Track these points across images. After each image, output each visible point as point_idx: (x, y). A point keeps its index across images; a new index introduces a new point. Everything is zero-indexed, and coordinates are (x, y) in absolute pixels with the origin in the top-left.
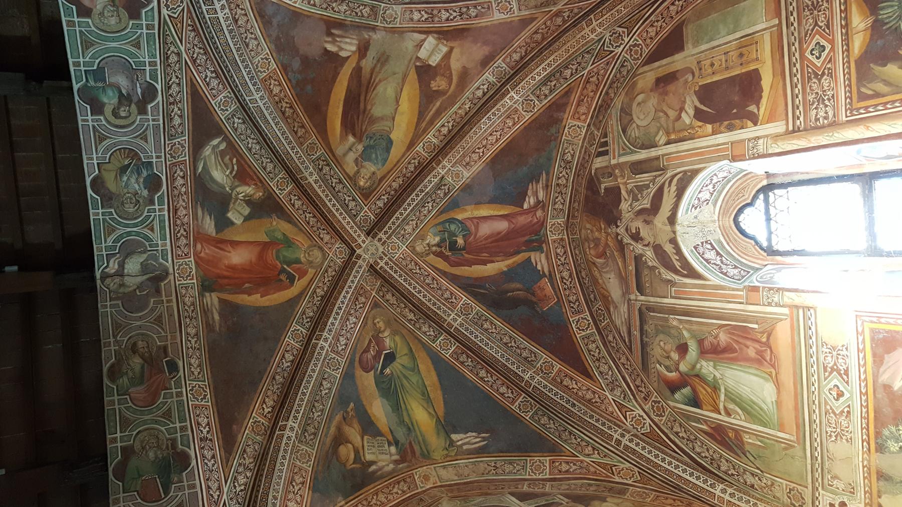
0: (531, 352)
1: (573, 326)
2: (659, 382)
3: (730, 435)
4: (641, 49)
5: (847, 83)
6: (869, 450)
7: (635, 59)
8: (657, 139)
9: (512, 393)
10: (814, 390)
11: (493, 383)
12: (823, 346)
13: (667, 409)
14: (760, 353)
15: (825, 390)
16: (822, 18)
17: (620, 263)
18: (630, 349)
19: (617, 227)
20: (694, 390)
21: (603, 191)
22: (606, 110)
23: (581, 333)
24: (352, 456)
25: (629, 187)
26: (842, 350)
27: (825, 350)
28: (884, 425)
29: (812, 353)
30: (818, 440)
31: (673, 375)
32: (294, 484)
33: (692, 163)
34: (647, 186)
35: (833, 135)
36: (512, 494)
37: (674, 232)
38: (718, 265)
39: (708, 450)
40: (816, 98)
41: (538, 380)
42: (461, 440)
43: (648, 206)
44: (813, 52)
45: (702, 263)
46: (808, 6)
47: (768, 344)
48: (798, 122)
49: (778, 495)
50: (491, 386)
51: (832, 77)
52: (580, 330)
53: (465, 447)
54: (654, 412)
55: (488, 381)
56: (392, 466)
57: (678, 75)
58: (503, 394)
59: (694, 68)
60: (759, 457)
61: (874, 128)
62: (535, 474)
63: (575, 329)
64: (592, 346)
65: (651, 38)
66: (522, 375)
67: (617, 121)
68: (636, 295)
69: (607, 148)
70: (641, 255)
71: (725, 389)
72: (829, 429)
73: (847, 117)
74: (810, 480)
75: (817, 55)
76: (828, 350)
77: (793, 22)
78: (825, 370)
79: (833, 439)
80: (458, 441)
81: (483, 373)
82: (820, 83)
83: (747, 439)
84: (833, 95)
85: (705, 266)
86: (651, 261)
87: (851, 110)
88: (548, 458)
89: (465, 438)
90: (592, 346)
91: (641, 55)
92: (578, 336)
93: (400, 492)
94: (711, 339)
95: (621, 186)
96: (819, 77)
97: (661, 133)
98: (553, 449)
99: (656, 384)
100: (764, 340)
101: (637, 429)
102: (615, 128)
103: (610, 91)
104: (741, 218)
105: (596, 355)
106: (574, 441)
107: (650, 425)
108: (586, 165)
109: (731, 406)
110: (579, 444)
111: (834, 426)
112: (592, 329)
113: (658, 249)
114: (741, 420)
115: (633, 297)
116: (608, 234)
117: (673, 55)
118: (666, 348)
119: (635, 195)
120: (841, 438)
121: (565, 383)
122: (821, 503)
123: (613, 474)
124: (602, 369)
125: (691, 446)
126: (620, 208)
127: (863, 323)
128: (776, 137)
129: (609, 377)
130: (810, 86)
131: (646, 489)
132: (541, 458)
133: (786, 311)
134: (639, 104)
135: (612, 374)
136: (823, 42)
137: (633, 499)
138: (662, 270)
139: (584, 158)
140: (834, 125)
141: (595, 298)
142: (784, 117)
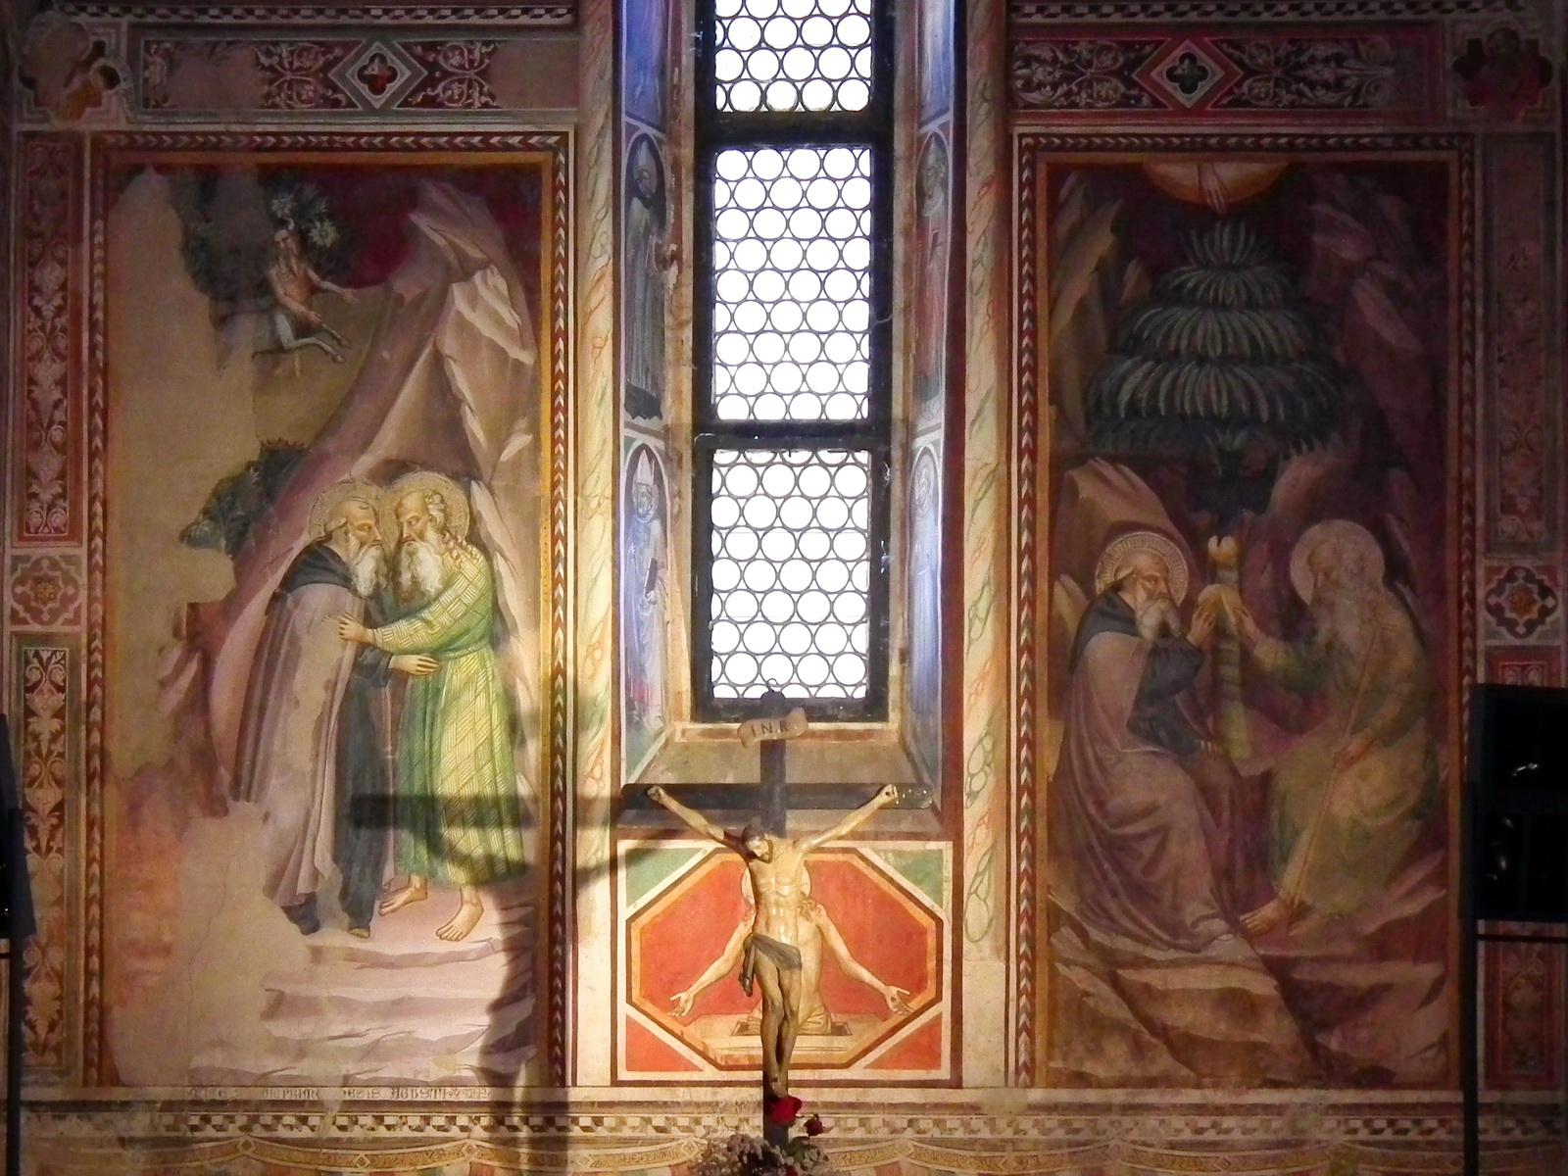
5: (1098, 141)
6: (259, 149)
10: (374, 12)
12: (486, 44)
15: (377, 43)
16: (1260, 88)
26: (481, 93)
29: (467, 12)
30: (250, 20)
35: (986, 100)
40: (1079, 61)
44: (1187, 62)
46: (1300, 52)
51: (1117, 105)
61: (985, 200)
72: (284, 50)
73: (1021, 136)
75: (1179, 72)
76: (477, 55)
77: (1275, 10)
78: (430, 47)
79: (263, 59)
82: (1111, 73)
84: (1075, 105)
87: (1034, 149)
96: (1123, 74)
111: (296, 64)
120: (271, 82)
122: (94, 19)
127: (548, 148)
130: (1108, 48)
136: (1203, 88)
140: (1008, 105)
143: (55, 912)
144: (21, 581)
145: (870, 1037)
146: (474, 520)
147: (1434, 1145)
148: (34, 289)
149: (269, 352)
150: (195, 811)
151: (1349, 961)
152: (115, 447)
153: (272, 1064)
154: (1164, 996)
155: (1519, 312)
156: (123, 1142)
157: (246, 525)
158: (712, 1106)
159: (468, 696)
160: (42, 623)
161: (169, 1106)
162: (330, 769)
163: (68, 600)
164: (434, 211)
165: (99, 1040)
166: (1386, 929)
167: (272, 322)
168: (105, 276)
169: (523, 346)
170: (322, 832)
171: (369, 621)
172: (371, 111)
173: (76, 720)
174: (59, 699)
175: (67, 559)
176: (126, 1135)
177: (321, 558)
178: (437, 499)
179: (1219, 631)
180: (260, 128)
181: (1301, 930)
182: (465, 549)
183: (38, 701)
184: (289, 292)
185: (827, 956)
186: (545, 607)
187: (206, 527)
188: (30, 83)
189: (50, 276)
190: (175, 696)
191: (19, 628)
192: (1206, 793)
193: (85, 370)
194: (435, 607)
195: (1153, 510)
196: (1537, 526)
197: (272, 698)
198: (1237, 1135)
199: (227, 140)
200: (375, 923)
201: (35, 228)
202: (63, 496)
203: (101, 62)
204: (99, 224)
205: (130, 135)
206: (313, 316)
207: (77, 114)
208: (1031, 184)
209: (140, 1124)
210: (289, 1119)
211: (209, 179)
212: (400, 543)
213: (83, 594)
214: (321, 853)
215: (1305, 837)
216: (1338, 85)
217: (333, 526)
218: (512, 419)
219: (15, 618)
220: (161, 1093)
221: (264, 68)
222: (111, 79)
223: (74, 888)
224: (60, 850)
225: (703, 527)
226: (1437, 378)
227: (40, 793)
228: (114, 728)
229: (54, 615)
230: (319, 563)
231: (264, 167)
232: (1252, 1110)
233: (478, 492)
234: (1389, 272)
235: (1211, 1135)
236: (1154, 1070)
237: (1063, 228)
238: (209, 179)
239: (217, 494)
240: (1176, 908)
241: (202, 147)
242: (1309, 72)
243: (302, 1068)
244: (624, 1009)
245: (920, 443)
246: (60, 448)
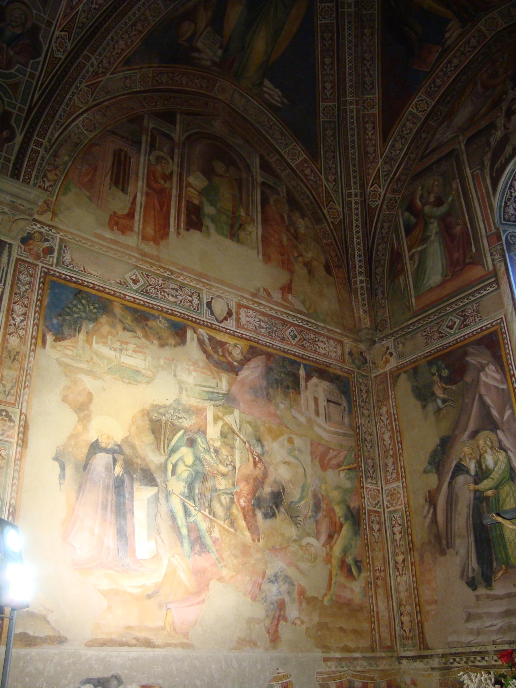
0: (372, 83)
1: (416, 100)
3: (399, 266)
9: (331, 94)
11: (327, 74)
12: (476, 304)
13: (395, 211)
17: (483, 110)
18: (423, 158)
23: (414, 109)
24: (188, 35)
26: (478, 317)
31: (419, 203)
32: (134, 28)
36: (262, 157)
38: (511, 195)
39: (383, 255)
41: (353, 108)
42: (269, 88)
45: (507, 183)
50: (324, 75)
52: (416, 107)
53: (266, 96)
54: (388, 202)
55: (325, 69)
56: (209, 63)
58: (324, 88)
62: (288, 156)
63: (414, 102)
64: (409, 125)
66: (348, 94)
72: (428, 329)
74: (395, 330)
76: (475, 307)
79: (424, 334)
80: (266, 87)
81: (328, 60)
83: (401, 278)
85: (505, 188)
86: (494, 139)
88: (305, 156)
89: (272, 90)
90: (409, 125)
92: (410, 109)
93: (199, 85)
98: (314, 155)
100: (467, 261)
101: (369, 198)
105: (405, 132)
106: (330, 163)
107: (378, 205)
109: (416, 258)
110: (330, 168)
112: (423, 115)
114: (411, 269)
115: (461, 138)
120: (426, 339)
121: (367, 126)
123: (327, 205)
124: (396, 144)
125: (380, 242)
129: (394, 154)
131: (332, 233)
132: (301, 151)
133: (491, 268)
135: (397, 155)
137: (318, 231)
138: (489, 154)
143: (406, 594)
144: (387, 496)
146: (500, 441)
148: (381, 415)
149: (436, 412)
150: (438, 555)
152: (405, 451)
153: (470, 638)
157: (439, 463)
159: (508, 499)
160: (394, 507)
162: (472, 533)
163: (399, 498)
167: (436, 402)
168: (396, 406)
169: (503, 383)
170: (473, 555)
171: (476, 483)
172: (451, 335)
173: (405, 532)
174: (400, 528)
175: (397, 487)
176: (433, 667)
177: (460, 467)
178: (488, 439)
180: (426, 352)
182: (499, 452)
184: (439, 393)
188: (374, 363)
189: (384, 410)
190: (428, 520)
191: (389, 510)
193: (395, 432)
194: (494, 473)
197: (453, 514)
199: (419, 358)
200: (493, 584)
201: (379, 399)
202: (394, 469)
203: (389, 351)
204: (393, 392)
205: (397, 367)
206: (446, 397)
207: (385, 367)
209: (435, 663)
212: (481, 455)
213: (402, 495)
214: (474, 563)
217: (461, 456)
218: (505, 406)
221: (424, 336)
222: (391, 354)
223: (410, 585)
224: (405, 574)
227: (398, 557)
229: (396, 503)
231: (428, 361)
233: (499, 432)
239: (431, 457)
241: (414, 362)
243: (481, 639)
246: (392, 456)
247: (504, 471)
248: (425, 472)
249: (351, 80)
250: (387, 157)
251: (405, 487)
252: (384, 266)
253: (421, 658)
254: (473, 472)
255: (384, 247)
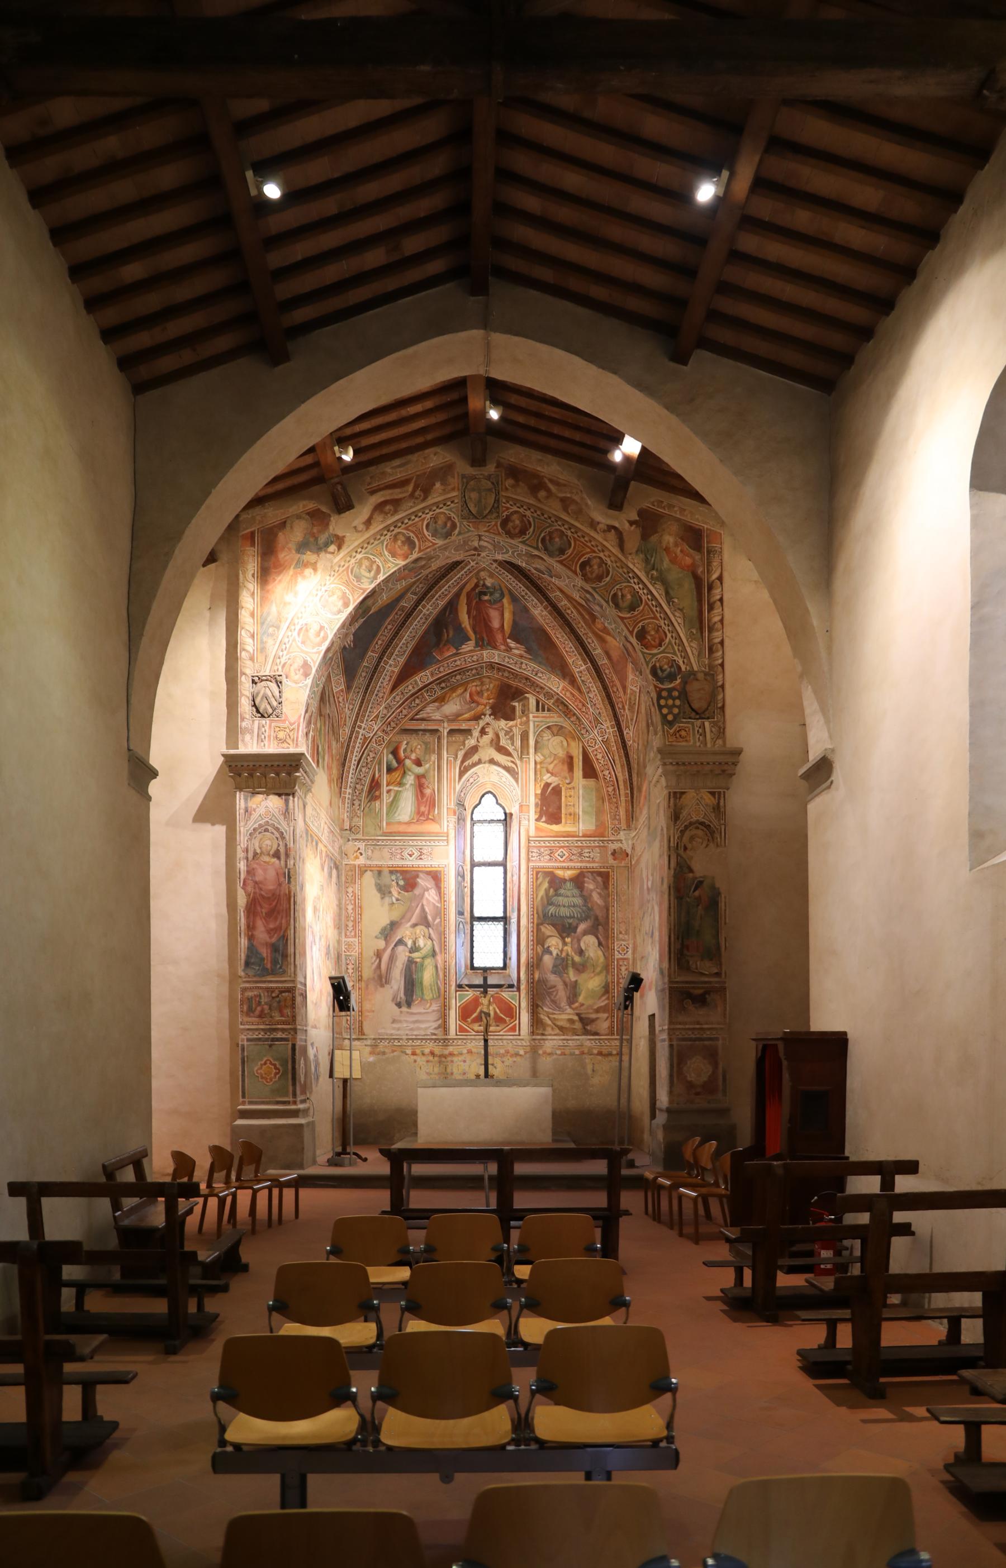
2: (396, 742)
4: (592, 747)
7: (588, 741)
8: (539, 754)
14: (423, 814)
17: (466, 716)
18: (412, 719)
19: (490, 715)
20: (396, 769)
21: (514, 704)
22: (564, 712)
25: (514, 729)
27: (430, 849)
28: (401, 874)
31: (402, 754)
33: (522, 779)
34: (513, 744)
37: (485, 763)
43: (501, 744)
47: (428, 819)
48: (532, 842)
49: (354, 820)
57: (571, 773)
59: (572, 784)
60: (370, 810)
64: (410, 687)
65: (596, 755)
67: (556, 722)
68: (447, 728)
69: (540, 710)
70: (471, 735)
71: (400, 791)
74: (367, 838)
83: (378, 803)
90: (410, 687)
91: (589, 746)
94: (426, 783)
95: (515, 722)
97: (542, 758)
99: (393, 739)
100: (430, 817)
102: (552, 720)
103: (575, 717)
104: (490, 795)
108: (533, 688)
109: (392, 794)
113: (474, 749)
115: (446, 725)
116: (485, 706)
117: (583, 769)
118: (417, 750)
119: (509, 732)
126: (502, 719)
128: (528, 831)
133: (445, 831)
134: (562, 742)
136: (564, 857)
139: (537, 686)
140: (528, 860)
141: (443, 688)
142: (537, 835)
145: (503, 1027)
146: (430, 934)
147: (607, 1046)
150: (378, 986)
151: (591, 1013)
153: (393, 1032)
154: (557, 1020)
155: (622, 898)
156: (366, 1045)
158: (474, 1039)
161: (374, 1039)
164: (421, 878)
165: (361, 1027)
166: (598, 1008)
171: (410, 952)
172: (410, 860)
174: (353, 966)
179: (568, 955)
181: (582, 1008)
183: (349, 967)
184: (395, 894)
185: (495, 1013)
186: (443, 950)
187: (380, 935)
188: (346, 855)
189: (350, 890)
192: (565, 984)
195: (555, 933)
196: (626, 936)
198: (571, 1044)
206: (399, 898)
207: (355, 861)
208: (533, 874)
209: (369, 1042)
210: (396, 1041)
211: (380, 873)
214: (402, 994)
215: (583, 992)
216: (589, 857)
219: (345, 952)
220: (373, 1037)
225: (472, 936)
226: (608, 910)
228: (363, 972)
229: (352, 951)
230: (401, 942)
232: (573, 1040)
234: (598, 890)
235: (566, 1044)
236: (556, 1033)
237: (539, 882)
238: (380, 873)
239: (382, 930)
240: (560, 1004)
241: (379, 867)
242: (584, 855)
244: (458, 1022)
245: (512, 921)
246: (352, 921)
247: (429, 951)
248: (376, 937)
249: (399, 651)
250: (388, 704)
251: (360, 943)
252: (364, 785)
253: (358, 1039)
254: (409, 946)
255: (367, 770)
